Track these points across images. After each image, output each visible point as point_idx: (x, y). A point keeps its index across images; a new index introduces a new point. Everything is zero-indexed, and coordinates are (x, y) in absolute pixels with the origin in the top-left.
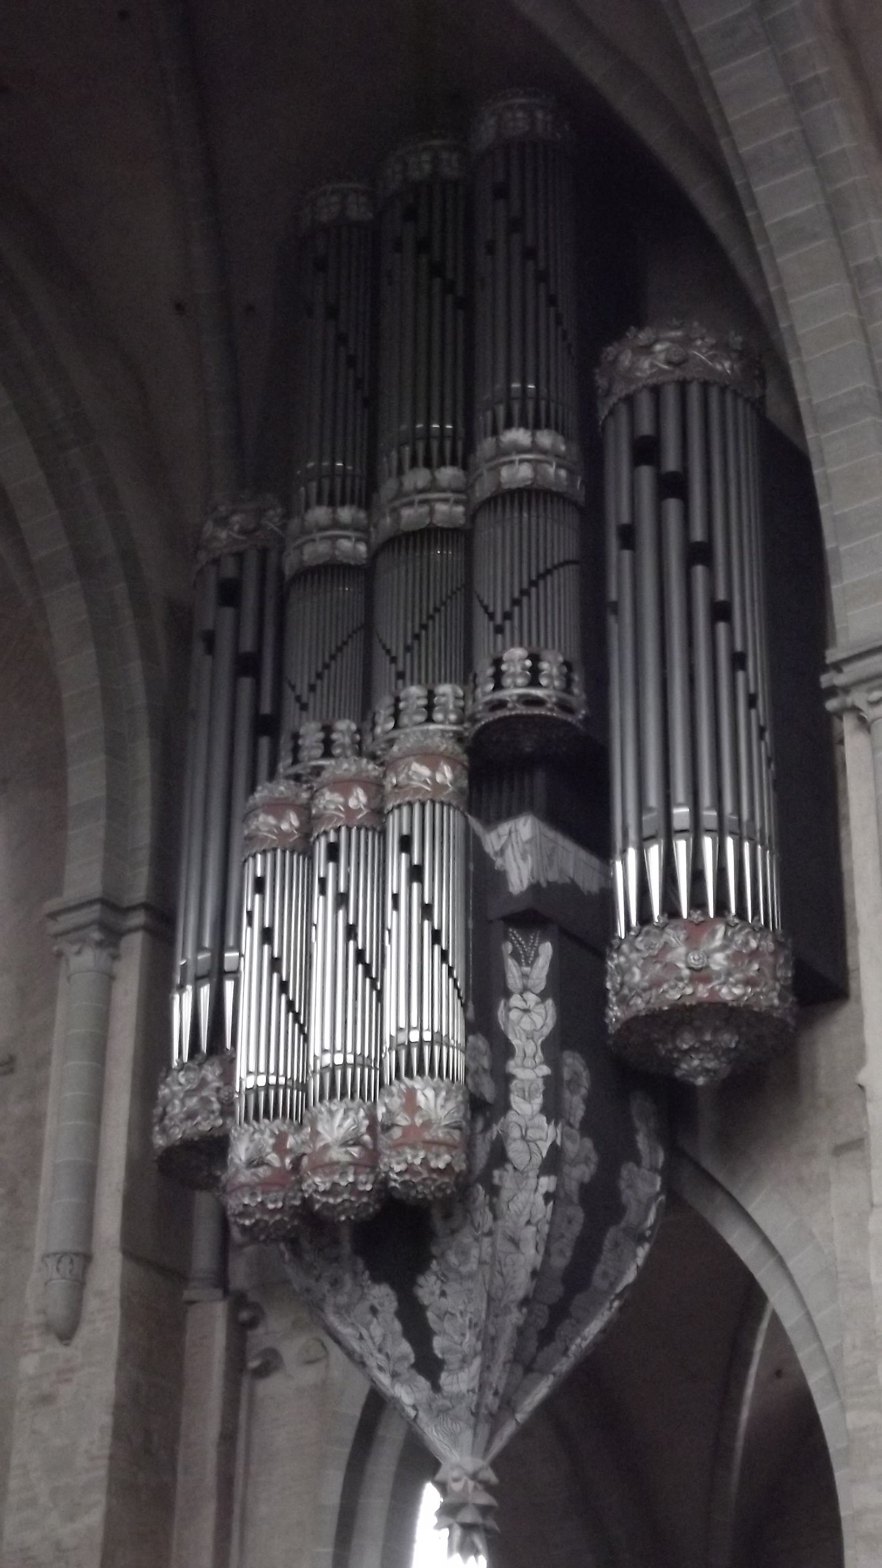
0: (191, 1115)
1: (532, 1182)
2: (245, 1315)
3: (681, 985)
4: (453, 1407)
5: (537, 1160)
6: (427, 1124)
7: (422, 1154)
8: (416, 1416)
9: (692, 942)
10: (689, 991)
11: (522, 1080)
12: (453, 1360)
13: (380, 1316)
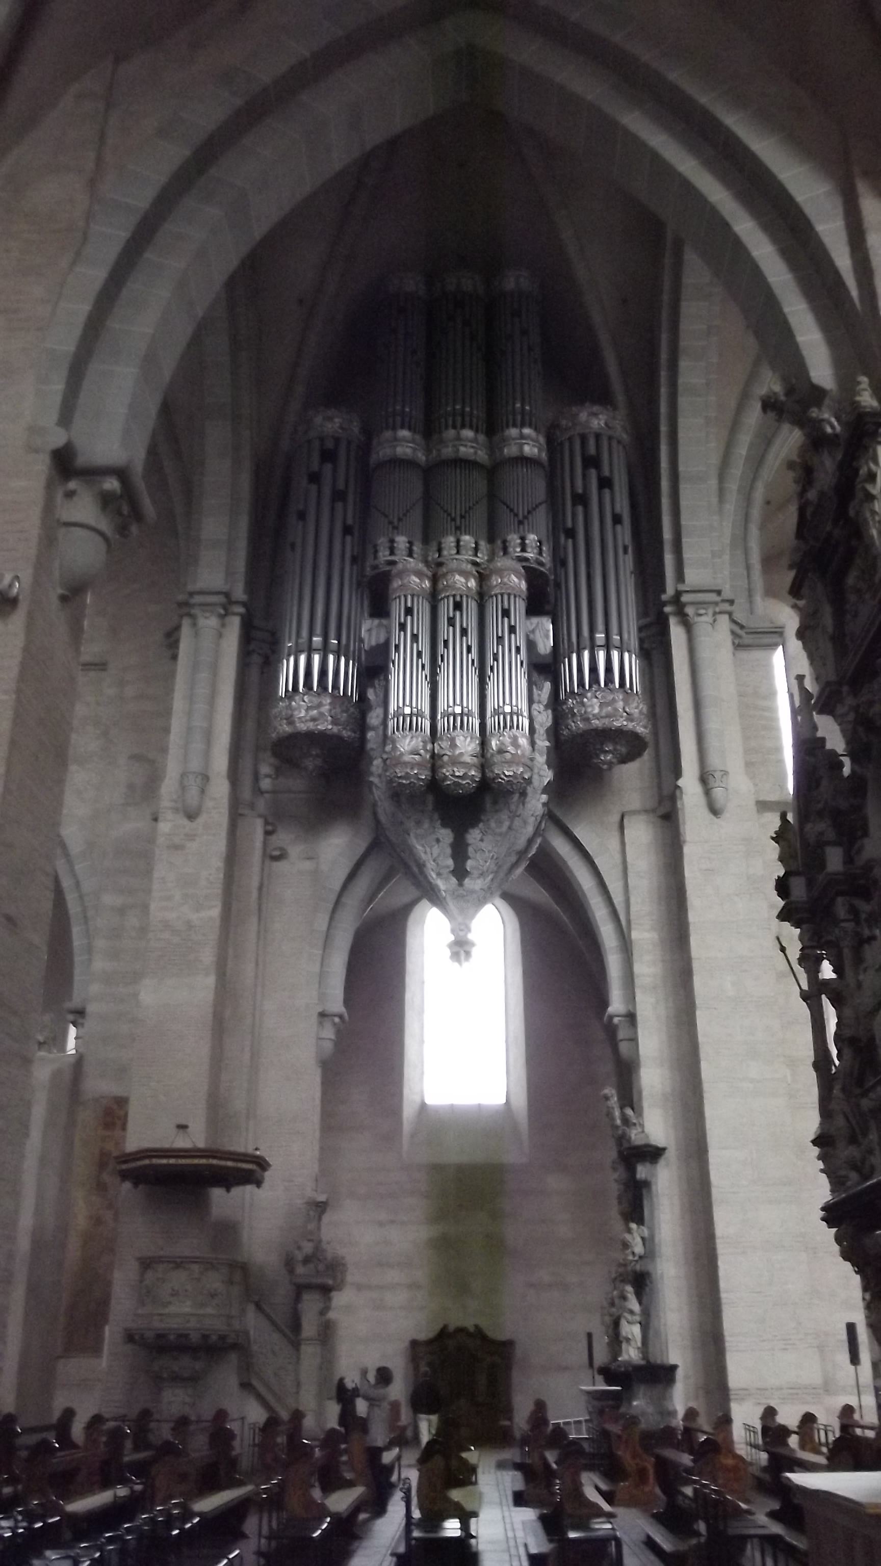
0: (313, 719)
1: (538, 796)
2: (270, 828)
3: (622, 719)
4: (467, 895)
5: (542, 787)
6: (523, 755)
7: (521, 770)
8: (446, 895)
9: (626, 702)
10: (625, 723)
11: (539, 745)
12: (476, 873)
13: (441, 844)
